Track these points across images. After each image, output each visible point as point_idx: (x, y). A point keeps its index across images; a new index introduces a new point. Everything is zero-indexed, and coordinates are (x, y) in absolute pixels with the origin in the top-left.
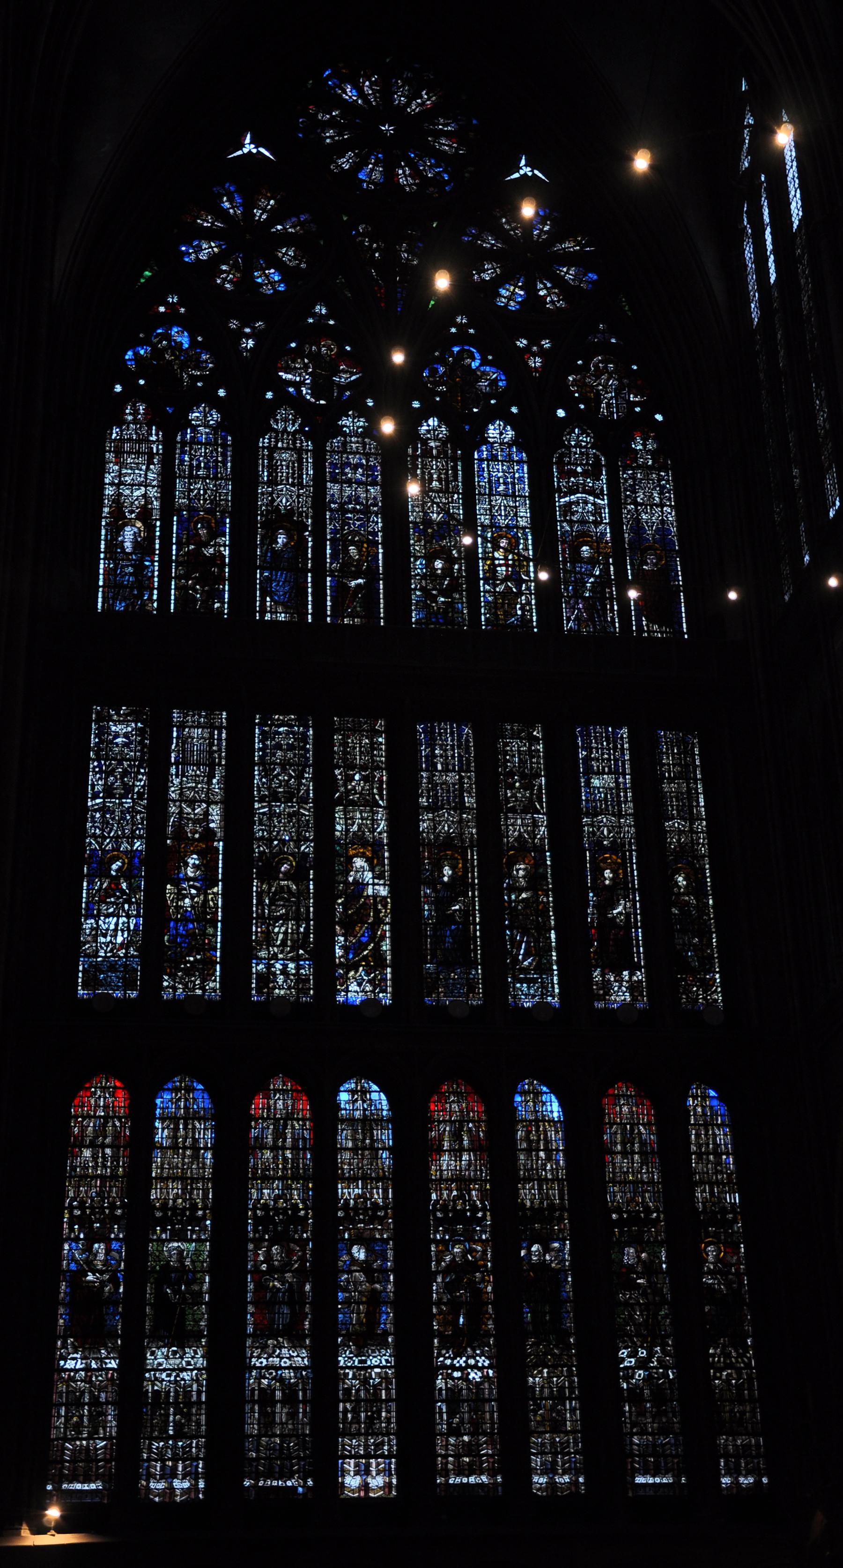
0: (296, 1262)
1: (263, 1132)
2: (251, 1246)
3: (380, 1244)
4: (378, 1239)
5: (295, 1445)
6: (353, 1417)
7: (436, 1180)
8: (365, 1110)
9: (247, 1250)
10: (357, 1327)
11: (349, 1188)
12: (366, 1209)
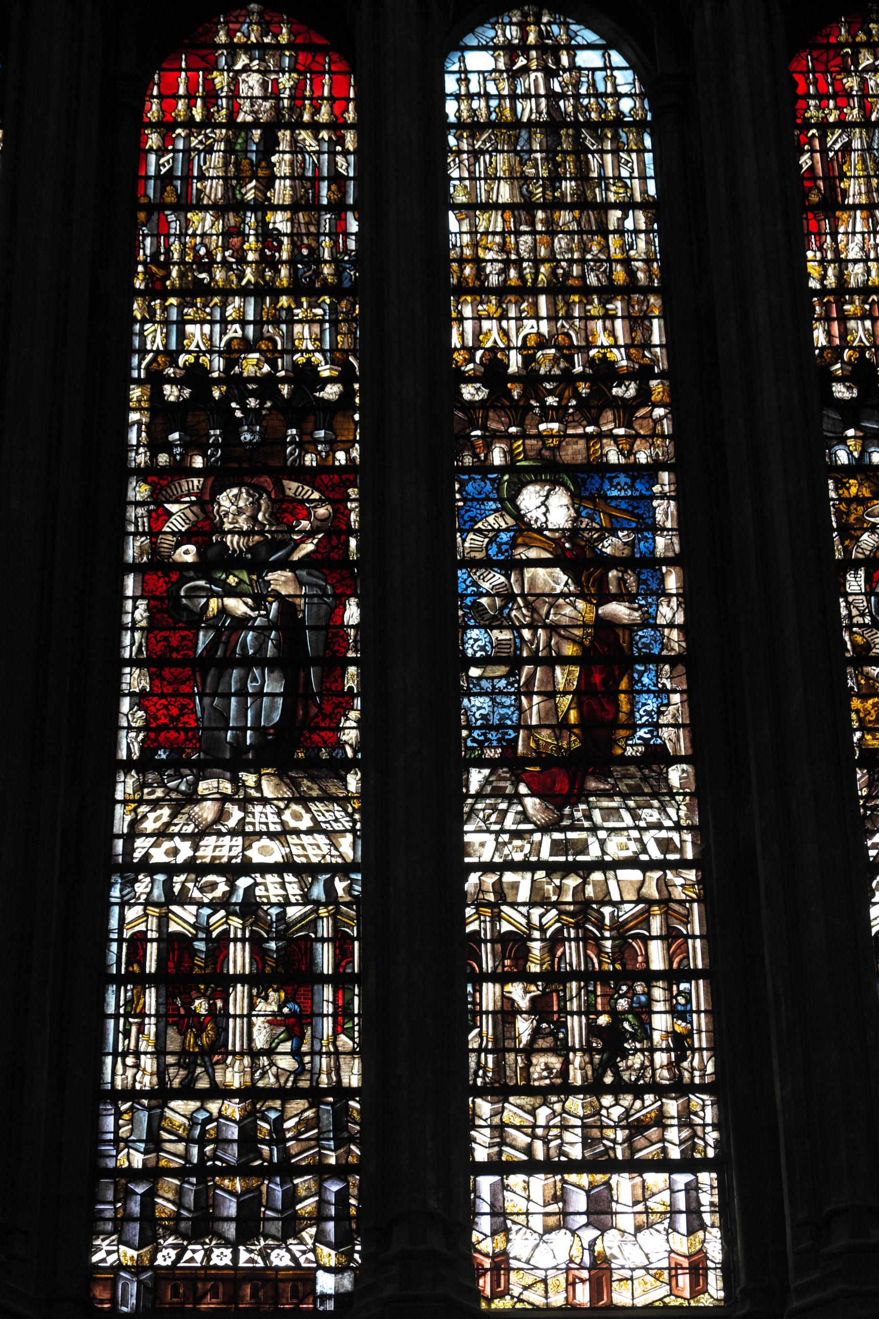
0: (309, 535)
1: (188, 162)
2: (139, 491)
3: (623, 479)
4: (618, 468)
5: (308, 1125)
6: (536, 1033)
7: (824, 291)
8: (552, 96)
9: (124, 503)
10: (545, 735)
11: (504, 316)
12: (567, 379)
